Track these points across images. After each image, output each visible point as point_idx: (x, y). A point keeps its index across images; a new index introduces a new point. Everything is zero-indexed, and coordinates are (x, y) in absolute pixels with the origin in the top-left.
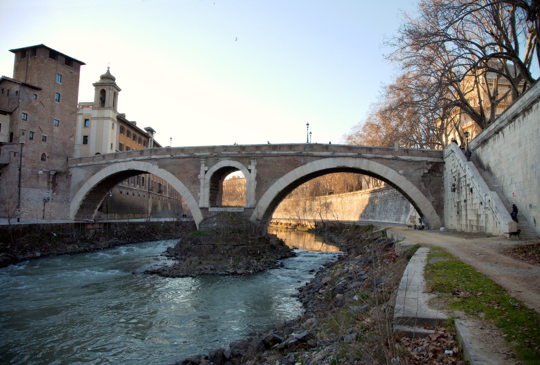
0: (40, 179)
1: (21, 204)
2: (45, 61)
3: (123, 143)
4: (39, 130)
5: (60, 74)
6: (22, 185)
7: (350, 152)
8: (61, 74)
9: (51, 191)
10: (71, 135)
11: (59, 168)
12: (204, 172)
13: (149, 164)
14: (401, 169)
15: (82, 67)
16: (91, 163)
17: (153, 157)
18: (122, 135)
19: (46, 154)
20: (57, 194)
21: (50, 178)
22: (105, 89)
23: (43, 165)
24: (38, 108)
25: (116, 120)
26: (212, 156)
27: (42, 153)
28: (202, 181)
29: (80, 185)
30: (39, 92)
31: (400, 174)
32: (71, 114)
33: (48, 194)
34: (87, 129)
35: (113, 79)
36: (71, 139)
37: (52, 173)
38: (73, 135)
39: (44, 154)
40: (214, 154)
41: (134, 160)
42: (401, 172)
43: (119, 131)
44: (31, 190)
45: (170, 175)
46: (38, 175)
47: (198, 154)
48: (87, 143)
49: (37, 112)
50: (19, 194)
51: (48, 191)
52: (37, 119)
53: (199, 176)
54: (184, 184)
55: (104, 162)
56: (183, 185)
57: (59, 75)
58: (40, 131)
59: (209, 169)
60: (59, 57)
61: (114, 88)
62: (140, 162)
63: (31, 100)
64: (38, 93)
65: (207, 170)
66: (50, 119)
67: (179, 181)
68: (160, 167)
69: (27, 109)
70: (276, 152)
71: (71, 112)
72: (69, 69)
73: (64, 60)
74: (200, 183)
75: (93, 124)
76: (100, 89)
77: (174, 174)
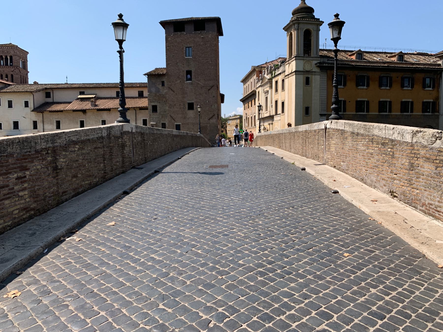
2: (170, 39)
5: (189, 46)
8: (190, 46)
10: (211, 116)
24: (167, 96)
30: (166, 77)
32: (209, 90)
35: (311, 10)
36: (211, 121)
38: (214, 115)
49: (166, 101)
52: (167, 108)
57: (189, 47)
58: (173, 121)
60: (186, 27)
61: (301, 26)
63: (159, 89)
64: (164, 79)
66: (182, 104)
69: (155, 99)
71: (209, 88)
72: (199, 35)
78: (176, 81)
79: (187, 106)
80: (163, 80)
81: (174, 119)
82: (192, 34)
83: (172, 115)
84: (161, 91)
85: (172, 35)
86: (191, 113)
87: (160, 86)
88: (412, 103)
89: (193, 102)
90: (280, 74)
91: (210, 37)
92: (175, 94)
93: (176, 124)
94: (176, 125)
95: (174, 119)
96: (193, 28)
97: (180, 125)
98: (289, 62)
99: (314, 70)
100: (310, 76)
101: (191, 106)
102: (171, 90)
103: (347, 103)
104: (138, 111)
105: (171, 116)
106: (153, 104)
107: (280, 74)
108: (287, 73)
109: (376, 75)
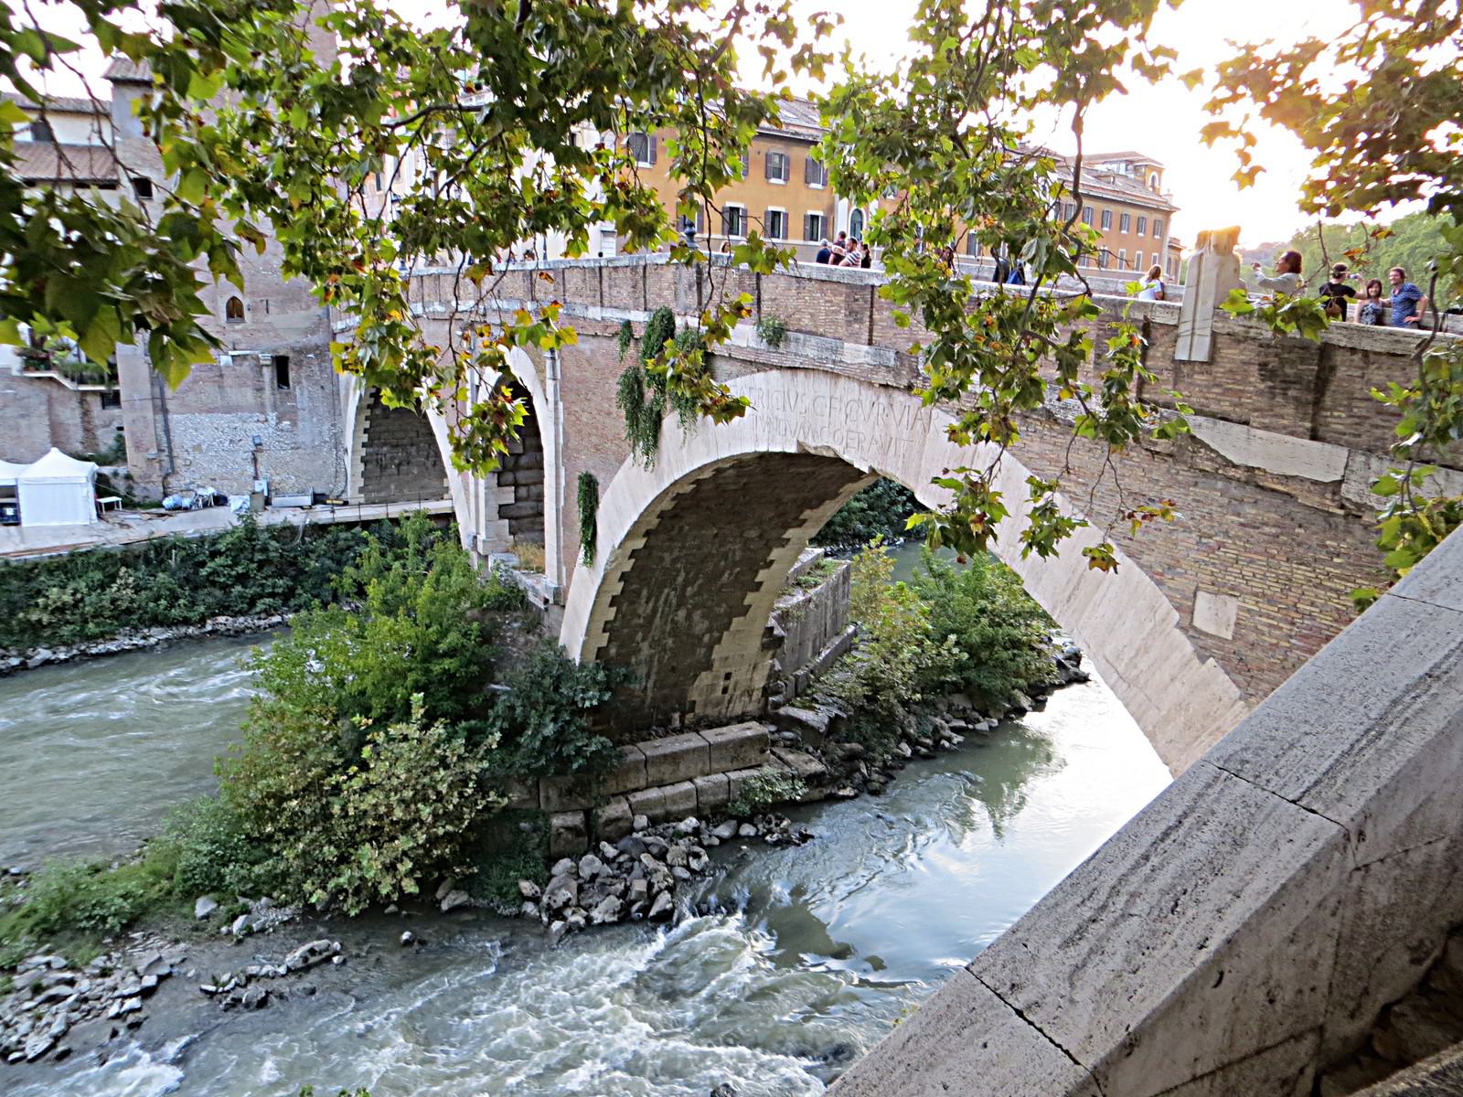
0: (228, 381)
1: (178, 462)
6: (170, 406)
7: (855, 338)
9: (272, 416)
11: (285, 343)
14: (1217, 588)
20: (294, 424)
21: (261, 375)
23: (238, 336)
27: (227, 297)
31: (1205, 646)
33: (262, 427)
37: (266, 358)
39: (234, 299)
42: (1214, 615)
46: (220, 368)
50: (167, 431)
51: (262, 418)
69: (144, 159)
70: (595, 313)
88: (786, 215)
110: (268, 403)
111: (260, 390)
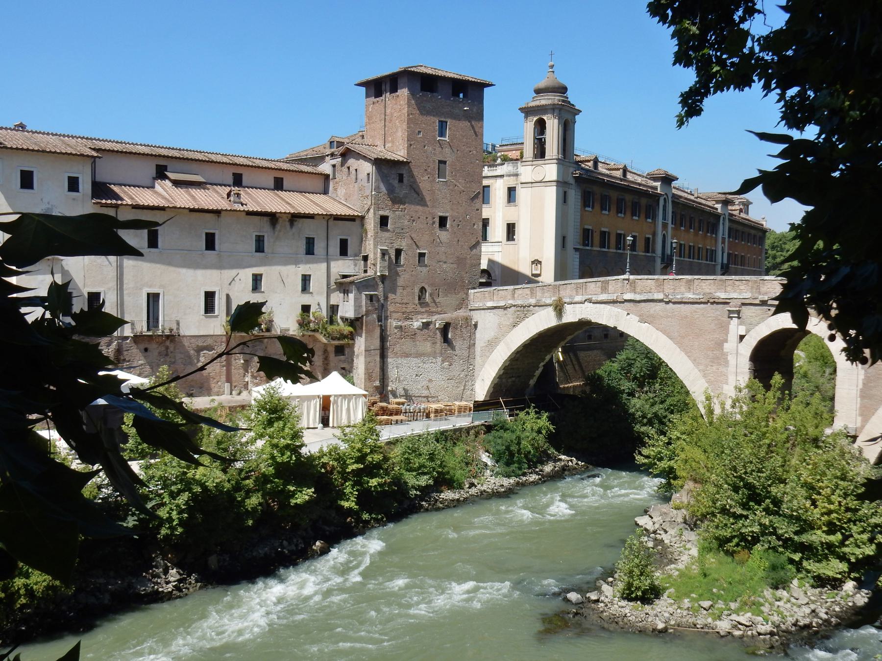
3: (590, 227)
4: (410, 242)
9: (439, 359)
12: (736, 339)
13: (619, 310)
15: (486, 90)
16: (511, 302)
17: (628, 296)
18: (590, 209)
19: (426, 287)
22: (545, 118)
25: (572, 181)
26: (757, 302)
28: (731, 359)
29: (492, 344)
34: (512, 209)
40: (761, 297)
41: (590, 301)
43: (579, 204)
44: (404, 361)
45: (663, 338)
47: (722, 295)
48: (514, 240)
51: (434, 360)
52: (406, 223)
53: (726, 345)
54: (694, 361)
55: (533, 301)
56: (690, 364)
58: (415, 247)
59: (748, 331)
62: (603, 305)
63: (393, 186)
65: (743, 334)
66: (430, 218)
67: (683, 353)
68: (642, 320)
72: (460, 105)
73: (449, 89)
74: (726, 363)
75: (522, 194)
76: (535, 119)
77: (671, 339)
78: (423, 177)
79: (437, 220)
80: (401, 172)
81: (416, 244)
82: (450, 100)
83: (412, 236)
84: (397, 190)
85: (418, 96)
86: (444, 235)
87: (395, 183)
89: (447, 215)
90: (502, 176)
91: (475, 110)
92: (419, 199)
93: (419, 251)
94: (419, 253)
95: (416, 244)
96: (451, 91)
97: (425, 253)
98: (534, 163)
99: (570, 182)
100: (567, 189)
101: (443, 221)
102: (413, 191)
103: (595, 234)
104: (331, 222)
105: (412, 238)
106: (382, 213)
107: (502, 176)
108: (523, 179)
109: (614, 195)
110: (438, 351)
111: (434, 343)
